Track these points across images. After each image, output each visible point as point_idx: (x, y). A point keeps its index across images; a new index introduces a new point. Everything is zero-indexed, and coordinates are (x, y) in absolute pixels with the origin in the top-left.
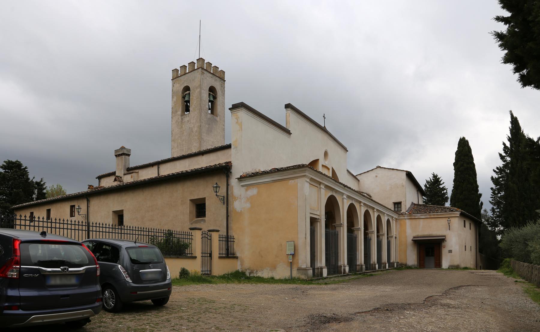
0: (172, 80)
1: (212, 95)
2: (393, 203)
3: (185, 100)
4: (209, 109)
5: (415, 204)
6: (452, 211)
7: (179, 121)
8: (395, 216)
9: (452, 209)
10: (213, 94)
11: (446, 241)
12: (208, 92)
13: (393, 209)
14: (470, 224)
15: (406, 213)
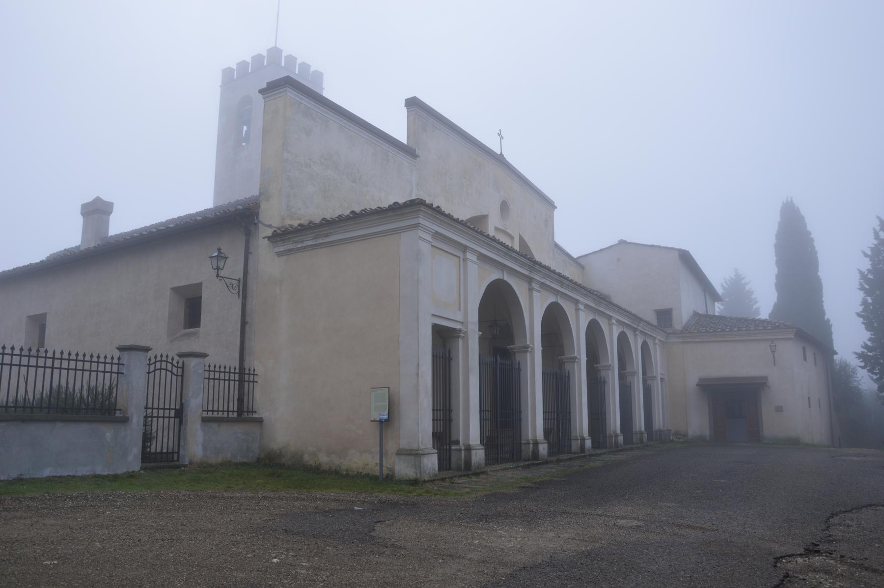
2: (655, 310)
13: (655, 323)
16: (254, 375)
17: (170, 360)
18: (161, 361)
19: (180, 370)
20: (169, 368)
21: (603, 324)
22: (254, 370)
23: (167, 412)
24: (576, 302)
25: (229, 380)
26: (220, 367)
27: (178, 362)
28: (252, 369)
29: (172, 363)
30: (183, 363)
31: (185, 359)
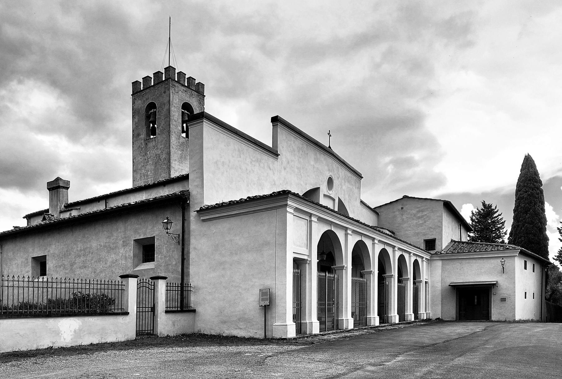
0: (131, 95)
1: (187, 114)
4: (183, 132)
5: (455, 242)
6: (508, 248)
7: (143, 147)
8: (426, 256)
9: (508, 247)
10: (188, 113)
11: (497, 287)
14: (534, 265)
16: (190, 287)
18: (143, 282)
21: (390, 250)
22: (191, 285)
23: (147, 309)
24: (373, 239)
26: (170, 284)
27: (151, 283)
29: (149, 283)
30: (154, 283)
31: (155, 281)
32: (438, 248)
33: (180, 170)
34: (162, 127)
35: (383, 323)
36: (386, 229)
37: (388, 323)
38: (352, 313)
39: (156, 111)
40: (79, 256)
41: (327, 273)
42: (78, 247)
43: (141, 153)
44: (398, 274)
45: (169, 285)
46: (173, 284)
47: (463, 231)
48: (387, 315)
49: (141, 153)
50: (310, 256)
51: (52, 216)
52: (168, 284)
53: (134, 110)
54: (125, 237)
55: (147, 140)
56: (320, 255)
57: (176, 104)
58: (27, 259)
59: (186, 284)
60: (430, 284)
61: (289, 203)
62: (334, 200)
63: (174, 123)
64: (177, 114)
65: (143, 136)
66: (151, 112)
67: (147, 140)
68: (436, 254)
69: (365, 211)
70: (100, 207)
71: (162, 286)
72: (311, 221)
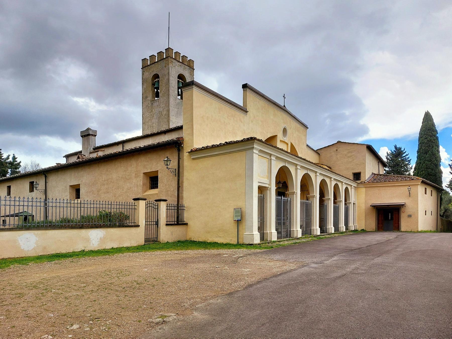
0: (141, 68)
1: (181, 82)
3: (155, 87)
4: (179, 95)
5: (375, 174)
6: (413, 179)
7: (150, 106)
8: (354, 184)
9: (413, 178)
10: (182, 81)
11: (405, 207)
12: (177, 79)
14: (431, 191)
15: (366, 182)
16: (184, 207)
17: (153, 203)
19: (157, 206)
20: (153, 206)
21: (328, 180)
22: (184, 205)
23: (152, 223)
25: (175, 209)
26: (169, 205)
27: (156, 204)
28: (183, 205)
30: (158, 204)
31: (159, 202)
32: (362, 179)
33: (176, 123)
34: (163, 92)
35: (323, 233)
36: (325, 165)
37: (327, 233)
38: (300, 225)
39: (159, 80)
40: (104, 185)
41: (282, 197)
42: (102, 178)
43: (148, 110)
44: (334, 198)
45: (168, 205)
46: (171, 204)
47: (380, 166)
48: (326, 227)
49: (148, 110)
50: (270, 184)
51: (84, 155)
52: (167, 204)
53: (143, 79)
54: (137, 171)
55: (153, 101)
56: (278, 184)
57: (174, 75)
58: (66, 187)
59: (180, 205)
60: (357, 204)
61: (255, 146)
62: (287, 144)
63: (172, 89)
64: (174, 82)
65: (150, 98)
66: (155, 80)
67: (153, 101)
68: (361, 183)
69: (310, 152)
70: (119, 149)
71: (163, 206)
72: (271, 159)
